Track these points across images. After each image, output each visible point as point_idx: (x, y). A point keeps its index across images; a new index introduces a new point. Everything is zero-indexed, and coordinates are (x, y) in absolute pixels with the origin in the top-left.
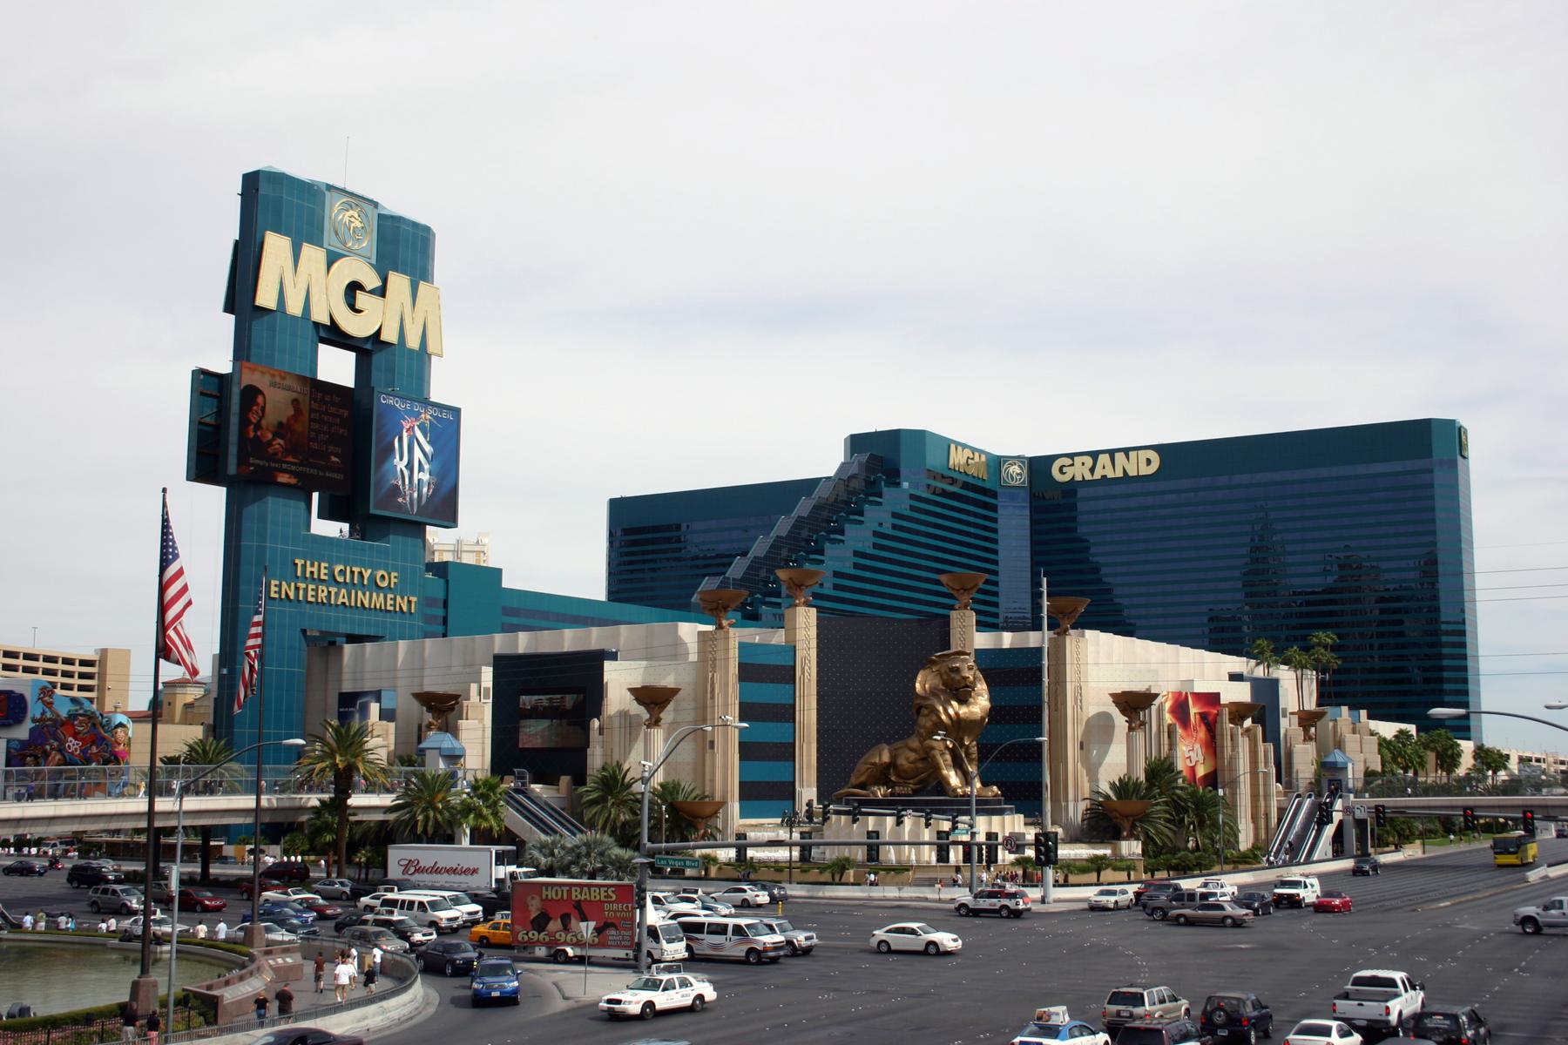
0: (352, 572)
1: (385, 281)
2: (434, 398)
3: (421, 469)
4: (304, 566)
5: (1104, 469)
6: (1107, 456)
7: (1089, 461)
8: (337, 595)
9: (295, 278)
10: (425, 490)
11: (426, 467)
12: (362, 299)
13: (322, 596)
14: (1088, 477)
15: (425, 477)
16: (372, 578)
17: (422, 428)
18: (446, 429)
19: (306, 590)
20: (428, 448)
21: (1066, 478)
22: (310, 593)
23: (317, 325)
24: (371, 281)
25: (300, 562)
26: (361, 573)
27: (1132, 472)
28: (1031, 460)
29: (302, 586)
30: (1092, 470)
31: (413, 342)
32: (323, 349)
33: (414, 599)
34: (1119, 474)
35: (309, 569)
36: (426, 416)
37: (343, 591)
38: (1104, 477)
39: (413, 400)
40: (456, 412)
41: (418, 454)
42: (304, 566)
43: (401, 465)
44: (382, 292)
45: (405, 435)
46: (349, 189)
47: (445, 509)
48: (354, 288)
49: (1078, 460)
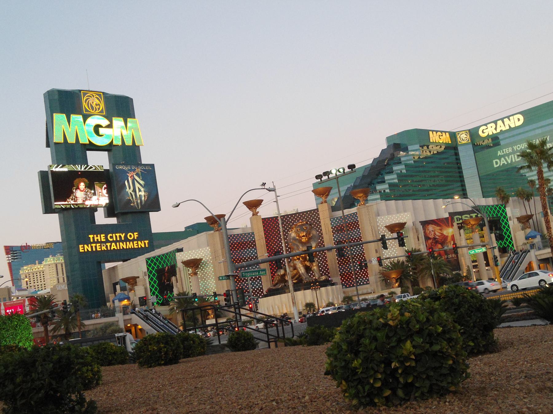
0: (116, 236)
1: (111, 122)
2: (144, 162)
3: (140, 190)
4: (93, 238)
5: (501, 127)
6: (501, 121)
7: (493, 125)
8: (111, 246)
9: (74, 128)
10: (143, 198)
11: (142, 189)
12: (101, 131)
13: (104, 248)
14: (495, 132)
15: (142, 193)
16: (126, 237)
17: (137, 175)
18: (149, 174)
19: (96, 247)
20: (142, 182)
21: (486, 135)
22: (98, 247)
23: (84, 145)
24: (104, 122)
25: (91, 236)
26: (120, 236)
27: (513, 126)
28: (469, 130)
29: (94, 245)
30: (496, 129)
31: (129, 142)
32: (89, 153)
33: (147, 242)
34: (508, 128)
35: (96, 238)
36: (139, 170)
37: (113, 244)
38: (501, 131)
39: (131, 165)
40: (152, 166)
41: (137, 185)
42: (93, 238)
43: (129, 191)
44: (110, 126)
45: (130, 179)
46: (90, 90)
47: (154, 204)
48: (97, 128)
49: (489, 126)
